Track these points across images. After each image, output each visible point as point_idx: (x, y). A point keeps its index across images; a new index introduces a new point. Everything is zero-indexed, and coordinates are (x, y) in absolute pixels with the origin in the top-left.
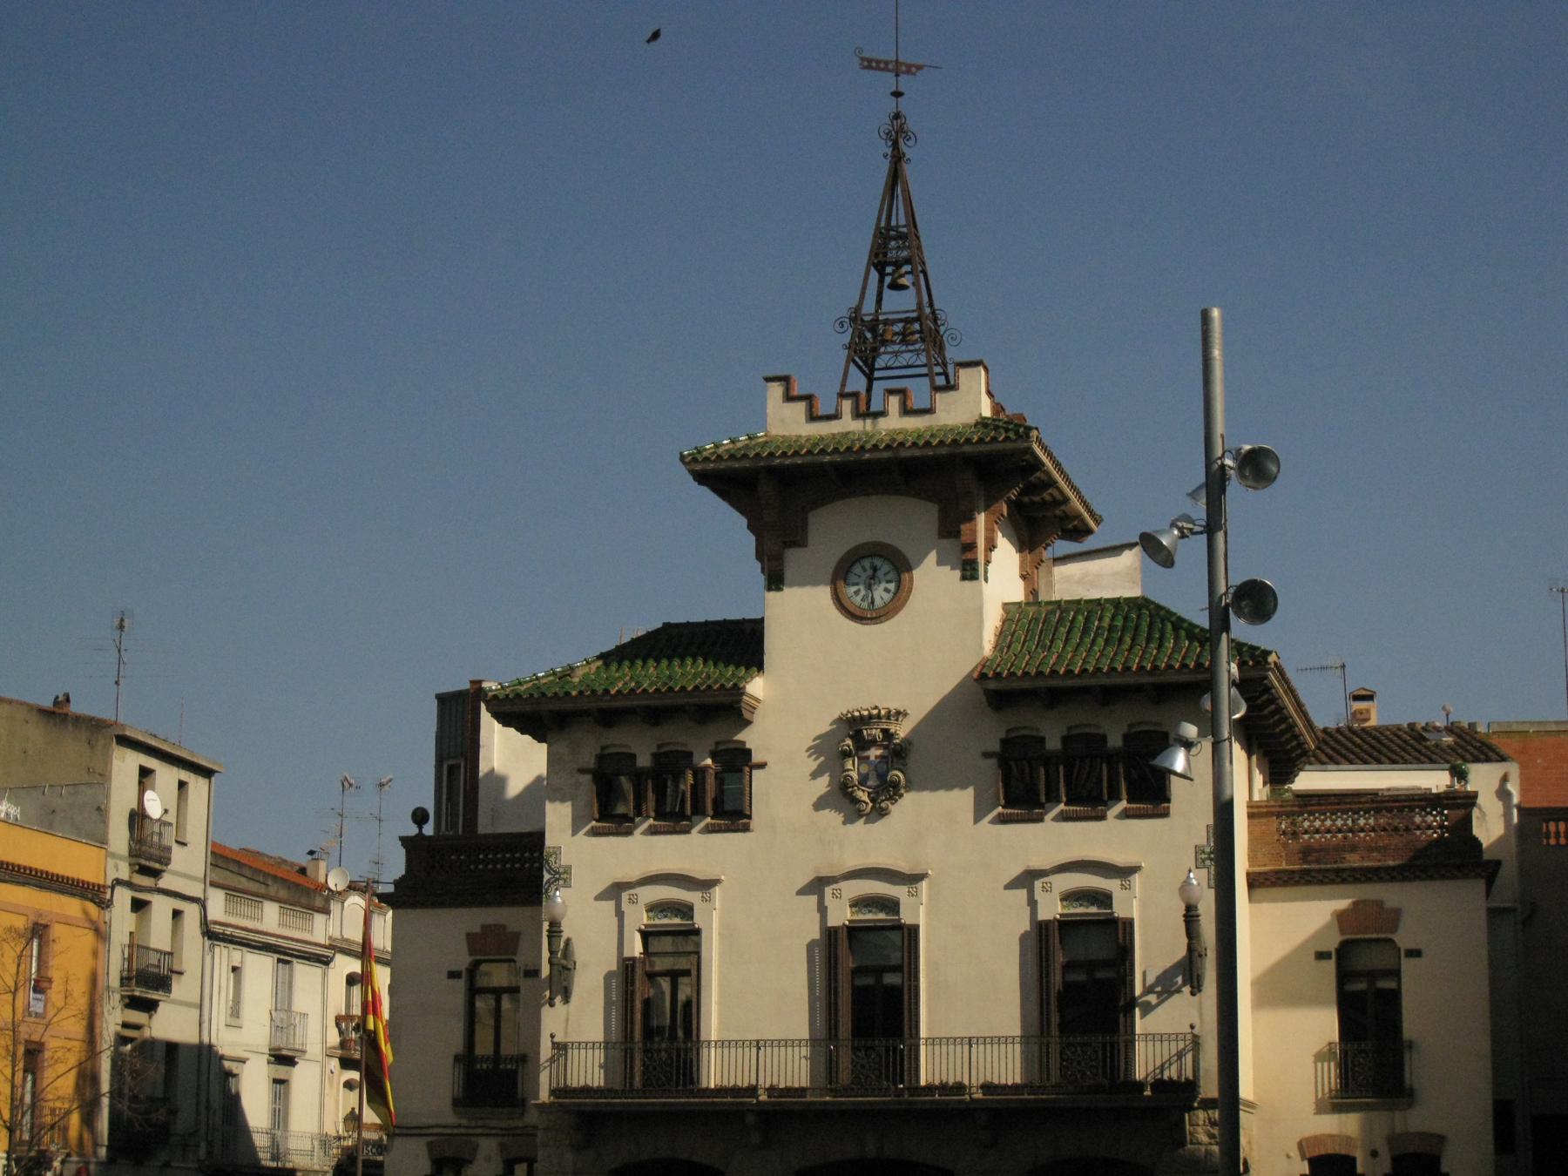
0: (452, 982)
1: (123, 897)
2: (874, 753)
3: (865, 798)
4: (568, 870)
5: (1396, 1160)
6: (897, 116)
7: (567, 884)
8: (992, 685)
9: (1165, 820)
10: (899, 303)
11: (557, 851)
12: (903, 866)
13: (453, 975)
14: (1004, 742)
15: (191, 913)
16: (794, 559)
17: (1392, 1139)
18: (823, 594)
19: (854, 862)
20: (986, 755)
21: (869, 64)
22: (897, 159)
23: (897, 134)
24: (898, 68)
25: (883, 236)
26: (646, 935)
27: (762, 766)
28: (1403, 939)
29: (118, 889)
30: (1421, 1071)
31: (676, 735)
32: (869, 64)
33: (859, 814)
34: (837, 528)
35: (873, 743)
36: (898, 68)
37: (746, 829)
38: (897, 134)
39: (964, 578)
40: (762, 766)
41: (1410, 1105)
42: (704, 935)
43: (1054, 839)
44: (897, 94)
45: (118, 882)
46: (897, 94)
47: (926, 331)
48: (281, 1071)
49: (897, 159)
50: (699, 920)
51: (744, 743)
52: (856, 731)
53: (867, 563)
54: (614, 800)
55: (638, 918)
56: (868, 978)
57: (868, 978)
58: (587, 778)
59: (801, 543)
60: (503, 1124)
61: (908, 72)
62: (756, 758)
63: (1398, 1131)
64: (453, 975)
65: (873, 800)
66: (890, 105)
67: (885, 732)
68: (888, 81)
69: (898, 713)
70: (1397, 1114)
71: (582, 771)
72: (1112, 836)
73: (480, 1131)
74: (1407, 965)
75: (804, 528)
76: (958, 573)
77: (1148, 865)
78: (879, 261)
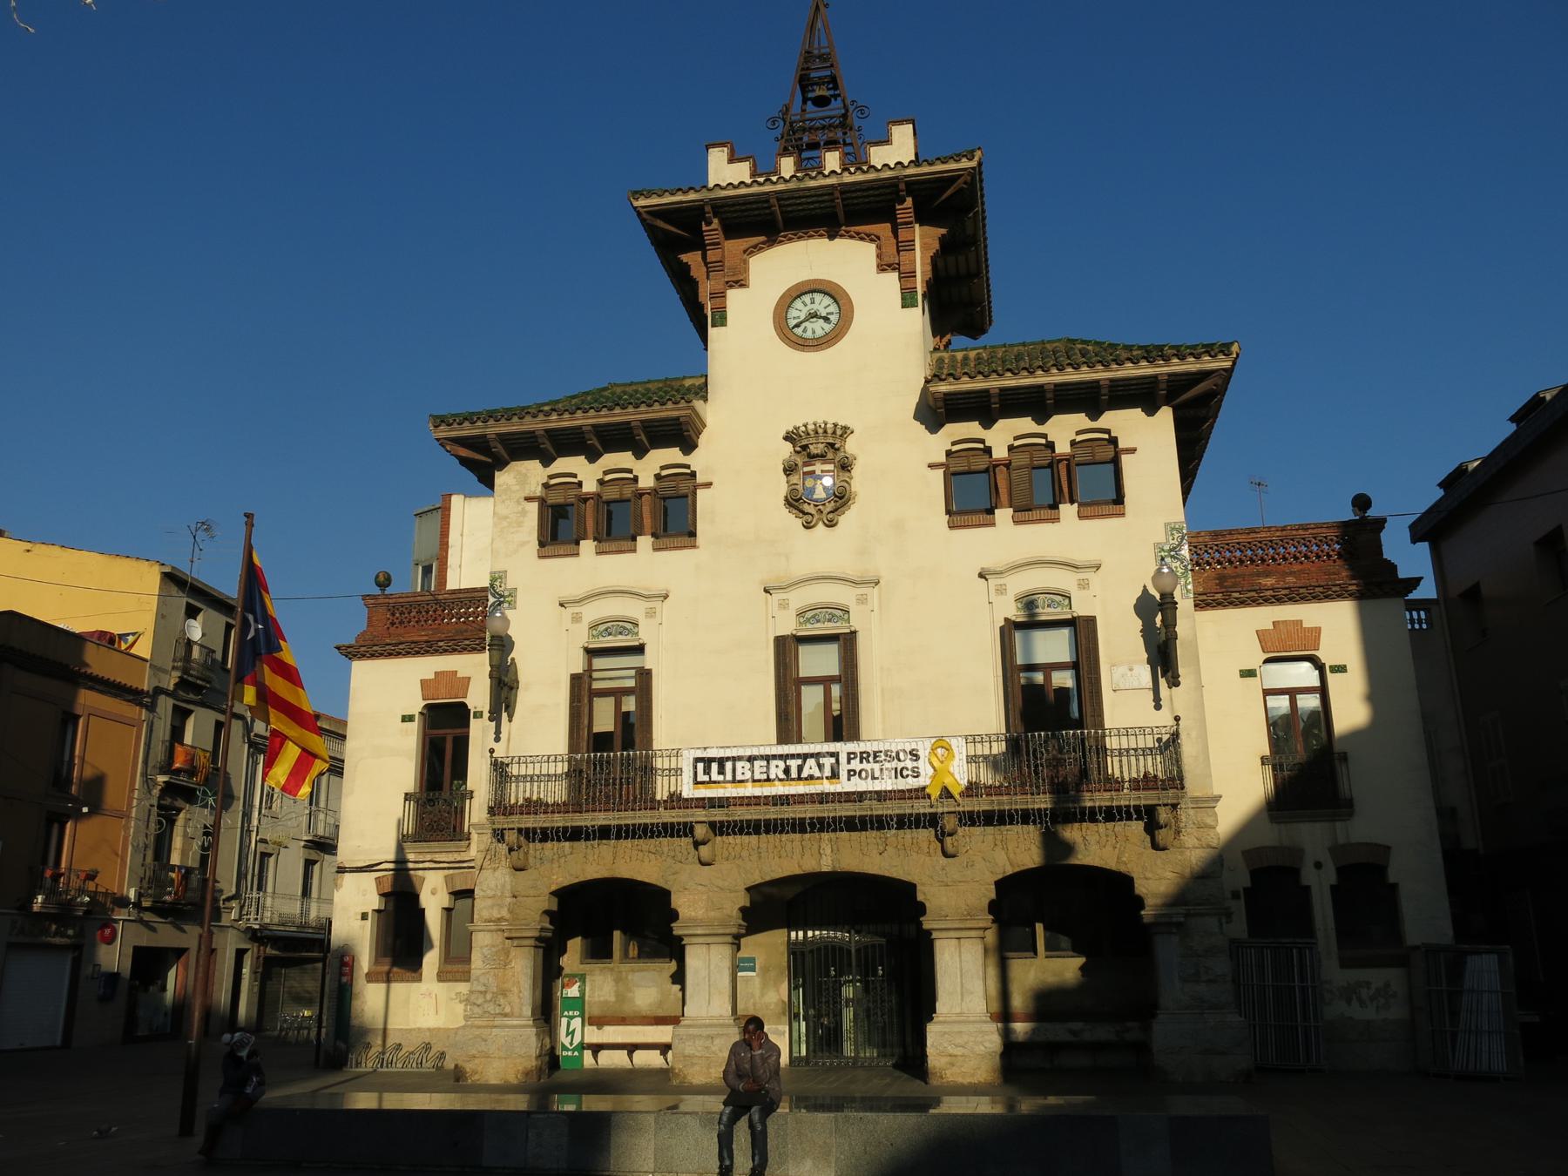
1: (165, 705)
2: (818, 467)
4: (513, 593)
5: (1340, 871)
7: (512, 605)
9: (1121, 520)
12: (851, 573)
13: (407, 719)
14: (949, 453)
15: (237, 726)
17: (1336, 850)
19: (800, 569)
25: (808, 56)
26: (592, 653)
29: (162, 699)
33: (808, 526)
35: (822, 456)
41: (1351, 815)
42: (647, 649)
43: (1006, 537)
45: (159, 691)
48: (313, 855)
50: (644, 635)
54: (560, 525)
55: (582, 637)
58: (534, 506)
60: (451, 857)
62: (700, 479)
63: (1341, 841)
64: (407, 719)
69: (845, 428)
70: (1338, 824)
71: (528, 499)
72: (1069, 532)
73: (427, 865)
74: (1332, 678)
78: (805, 83)
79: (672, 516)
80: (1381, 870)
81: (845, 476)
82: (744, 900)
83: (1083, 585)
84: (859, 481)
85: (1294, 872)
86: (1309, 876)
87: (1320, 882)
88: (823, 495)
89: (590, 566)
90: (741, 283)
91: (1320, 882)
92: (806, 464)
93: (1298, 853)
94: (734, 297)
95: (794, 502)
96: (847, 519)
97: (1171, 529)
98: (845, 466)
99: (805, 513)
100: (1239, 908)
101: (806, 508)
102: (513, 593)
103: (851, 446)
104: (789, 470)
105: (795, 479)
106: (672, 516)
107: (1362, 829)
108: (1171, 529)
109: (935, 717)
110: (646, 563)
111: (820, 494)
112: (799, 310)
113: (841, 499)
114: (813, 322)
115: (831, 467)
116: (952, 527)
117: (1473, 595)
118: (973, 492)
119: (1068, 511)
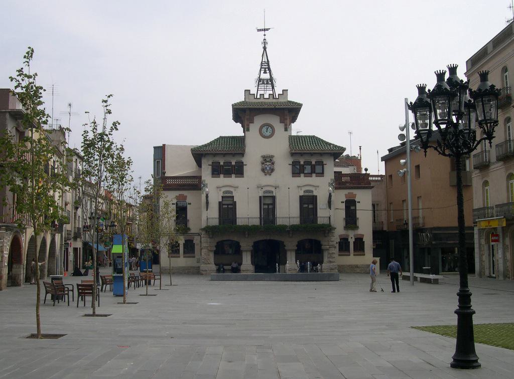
0: (174, 205)
2: (268, 163)
4: (207, 184)
6: (265, 39)
10: (267, 76)
11: (204, 181)
16: (251, 126)
20: (289, 164)
21: (259, 30)
22: (265, 48)
23: (265, 42)
24: (265, 30)
27: (246, 165)
28: (357, 200)
30: (360, 223)
31: (228, 159)
32: (259, 30)
33: (266, 175)
34: (259, 121)
35: (269, 162)
36: (265, 30)
37: (243, 177)
38: (265, 42)
40: (246, 165)
43: (302, 180)
44: (265, 35)
46: (265, 35)
47: (271, 81)
49: (265, 48)
50: (234, 194)
53: (266, 127)
54: (217, 171)
56: (268, 204)
57: (268, 204)
59: (253, 123)
61: (267, 30)
62: (244, 163)
66: (263, 37)
68: (263, 32)
72: (314, 180)
77: (321, 186)
79: (238, 170)
80: (362, 239)
82: (253, 244)
83: (316, 189)
84: (276, 167)
85: (347, 239)
86: (350, 240)
87: (351, 241)
89: (222, 180)
90: (252, 123)
91: (351, 241)
93: (348, 236)
94: (251, 125)
95: (263, 170)
96: (273, 174)
97: (331, 180)
98: (273, 164)
100: (337, 246)
101: (266, 171)
102: (207, 184)
103: (274, 159)
104: (263, 163)
106: (238, 170)
107: (360, 232)
108: (331, 180)
109: (288, 212)
110: (233, 180)
111: (268, 169)
112: (264, 129)
113: (272, 170)
114: (267, 132)
116: (293, 177)
117: (391, 176)
118: (298, 170)
119: (314, 175)
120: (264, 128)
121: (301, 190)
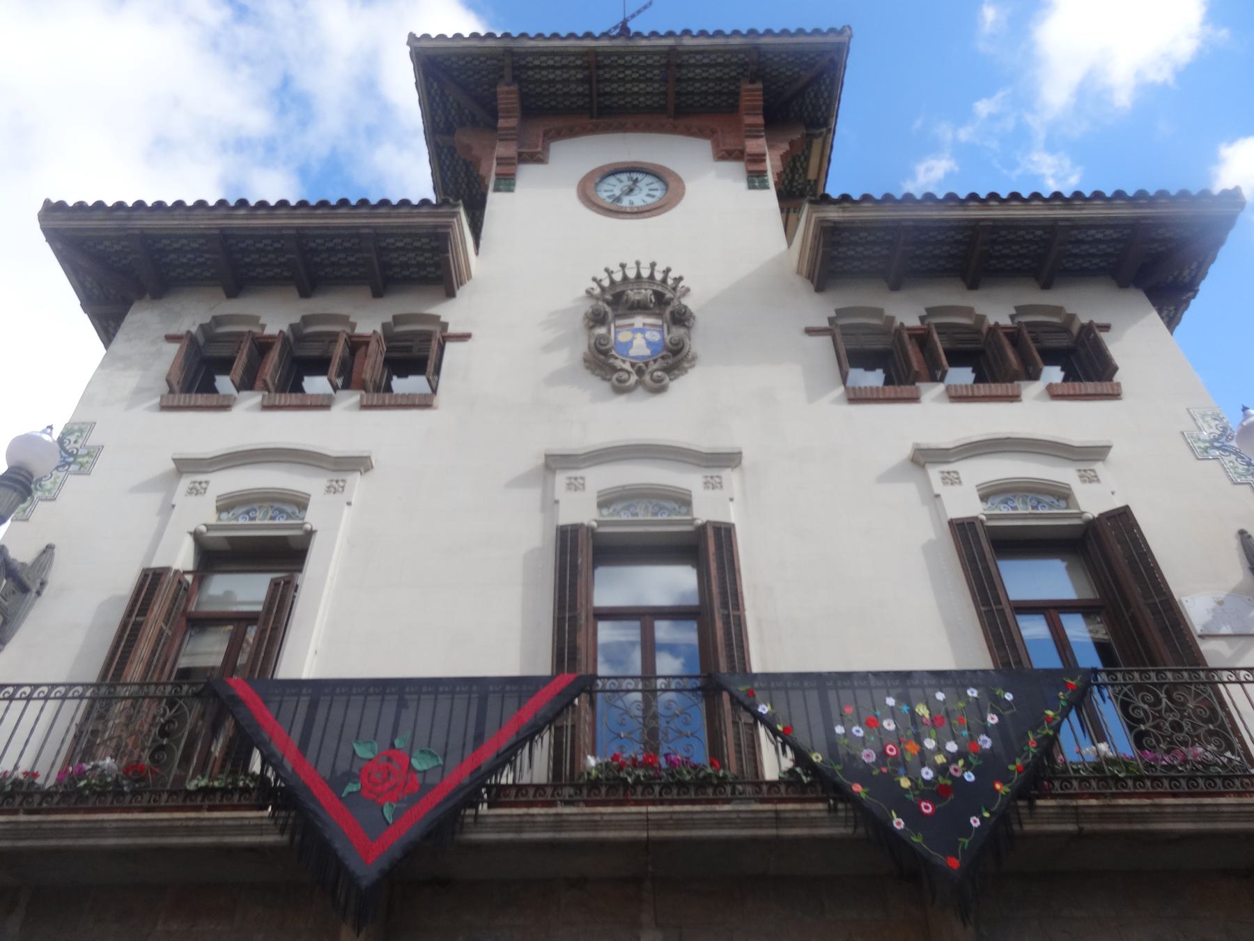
3: (627, 366)
8: (833, 214)
18: (569, 197)
20: (810, 331)
27: (465, 337)
39: (751, 186)
40: (465, 337)
50: (312, 518)
51: (439, 317)
52: (617, 299)
53: (624, 177)
62: (452, 329)
65: (640, 372)
67: (659, 296)
75: (546, 149)
76: (743, 184)
81: (678, 332)
88: (647, 352)
92: (617, 316)
99: (615, 370)
104: (597, 319)
105: (602, 331)
115: (659, 322)
120: (612, 180)
121: (952, 479)
